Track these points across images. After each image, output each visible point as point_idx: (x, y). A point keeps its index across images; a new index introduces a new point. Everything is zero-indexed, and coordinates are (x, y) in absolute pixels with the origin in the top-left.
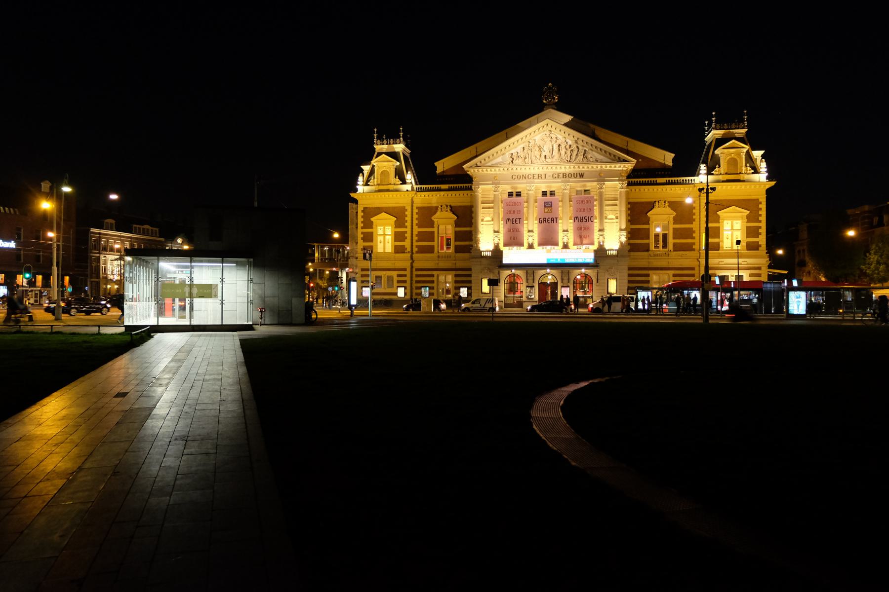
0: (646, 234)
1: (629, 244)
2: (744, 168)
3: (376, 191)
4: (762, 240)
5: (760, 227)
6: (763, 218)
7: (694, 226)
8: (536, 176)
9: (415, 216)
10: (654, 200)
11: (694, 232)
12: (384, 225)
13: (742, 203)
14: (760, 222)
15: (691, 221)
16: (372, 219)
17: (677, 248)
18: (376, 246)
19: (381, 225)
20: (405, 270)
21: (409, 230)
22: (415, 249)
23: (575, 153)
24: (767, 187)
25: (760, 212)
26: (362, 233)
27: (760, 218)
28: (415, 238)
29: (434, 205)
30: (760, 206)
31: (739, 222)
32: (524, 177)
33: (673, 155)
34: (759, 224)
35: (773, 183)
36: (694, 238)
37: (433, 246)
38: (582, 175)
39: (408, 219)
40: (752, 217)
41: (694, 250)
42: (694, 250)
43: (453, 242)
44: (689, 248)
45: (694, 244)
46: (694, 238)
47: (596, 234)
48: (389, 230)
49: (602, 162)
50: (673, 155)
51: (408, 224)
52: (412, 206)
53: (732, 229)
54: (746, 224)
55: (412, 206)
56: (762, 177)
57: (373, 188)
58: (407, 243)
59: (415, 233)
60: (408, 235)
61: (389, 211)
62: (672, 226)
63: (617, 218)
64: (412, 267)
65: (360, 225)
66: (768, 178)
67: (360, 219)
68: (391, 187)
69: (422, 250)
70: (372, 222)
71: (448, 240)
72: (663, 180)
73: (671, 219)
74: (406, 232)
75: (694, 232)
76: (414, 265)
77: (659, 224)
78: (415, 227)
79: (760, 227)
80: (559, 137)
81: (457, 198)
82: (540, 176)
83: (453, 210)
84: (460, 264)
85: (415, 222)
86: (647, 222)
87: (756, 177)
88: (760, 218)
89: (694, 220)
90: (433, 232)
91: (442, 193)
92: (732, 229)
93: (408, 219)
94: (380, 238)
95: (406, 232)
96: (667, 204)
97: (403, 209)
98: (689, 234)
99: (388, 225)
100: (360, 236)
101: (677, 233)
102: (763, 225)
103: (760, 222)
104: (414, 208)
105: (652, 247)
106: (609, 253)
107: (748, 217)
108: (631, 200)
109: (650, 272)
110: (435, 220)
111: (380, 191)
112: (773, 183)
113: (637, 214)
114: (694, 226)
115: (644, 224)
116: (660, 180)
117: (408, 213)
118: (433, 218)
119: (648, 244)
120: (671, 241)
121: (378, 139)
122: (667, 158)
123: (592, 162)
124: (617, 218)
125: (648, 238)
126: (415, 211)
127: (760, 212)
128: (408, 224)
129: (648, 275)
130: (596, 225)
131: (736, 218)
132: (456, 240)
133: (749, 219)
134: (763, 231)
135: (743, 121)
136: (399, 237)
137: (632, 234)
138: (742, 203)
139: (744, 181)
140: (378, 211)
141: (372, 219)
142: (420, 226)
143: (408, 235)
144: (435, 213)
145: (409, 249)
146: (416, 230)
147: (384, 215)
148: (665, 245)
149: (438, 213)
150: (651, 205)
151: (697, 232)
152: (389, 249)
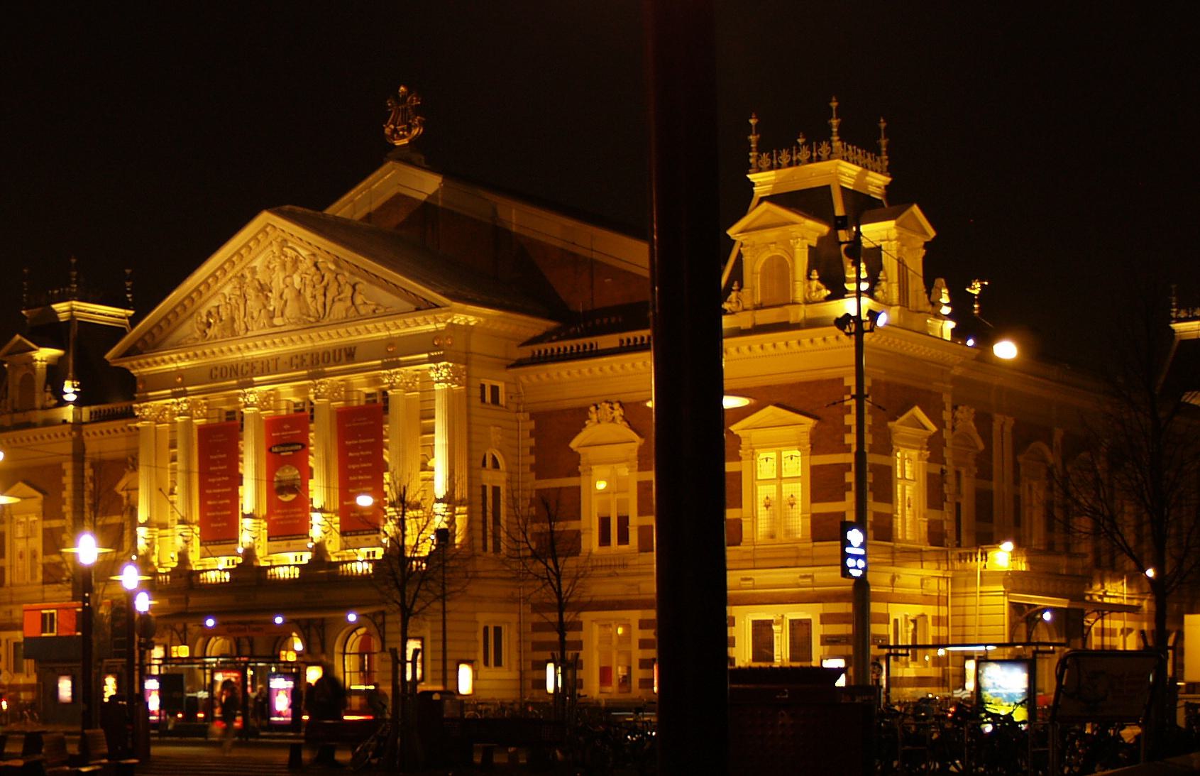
29: (122, 455)
86: (573, 465)
92: (780, 477)
126: (89, 472)
150: (577, 418)
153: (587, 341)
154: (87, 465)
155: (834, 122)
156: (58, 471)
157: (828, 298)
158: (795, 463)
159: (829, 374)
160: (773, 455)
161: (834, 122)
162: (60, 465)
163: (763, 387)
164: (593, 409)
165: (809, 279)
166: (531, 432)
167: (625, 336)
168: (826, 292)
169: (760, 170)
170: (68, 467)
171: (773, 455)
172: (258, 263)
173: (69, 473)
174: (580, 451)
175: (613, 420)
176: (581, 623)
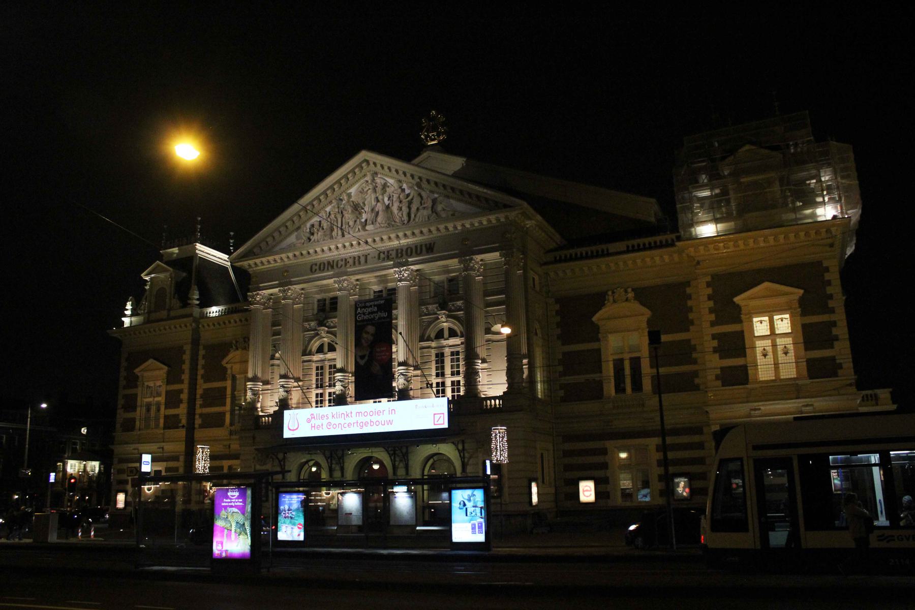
0: (595, 360)
4: (842, 351)
5: (834, 324)
6: (838, 301)
8: (351, 261)
9: (201, 362)
14: (832, 311)
15: (685, 324)
21: (185, 386)
22: (198, 421)
27: (831, 304)
28: (199, 402)
30: (827, 276)
32: (330, 265)
34: (833, 317)
36: (695, 362)
41: (696, 388)
42: (696, 388)
49: (464, 216)
51: (186, 377)
58: (182, 411)
59: (199, 392)
60: (184, 396)
72: (621, 246)
74: (181, 391)
75: (694, 349)
77: (624, 334)
78: (200, 381)
79: (834, 324)
80: (391, 181)
82: (356, 260)
85: (201, 372)
86: (594, 333)
88: (831, 304)
89: (692, 323)
90: (225, 388)
93: (186, 367)
95: (181, 391)
96: (631, 295)
98: (685, 353)
102: (840, 316)
103: (832, 311)
105: (610, 388)
107: (802, 302)
109: (609, 444)
110: (228, 366)
116: (613, 247)
117: (187, 357)
123: (447, 220)
126: (202, 352)
127: (829, 290)
128: (186, 377)
129: (604, 452)
134: (842, 331)
141: (136, 371)
142: (207, 379)
145: (184, 421)
148: (637, 386)
150: (598, 300)
153: (604, 247)
154: (201, 347)
156: (181, 350)
158: (783, 324)
160: (766, 318)
162: (182, 347)
164: (610, 293)
166: (557, 312)
170: (188, 348)
171: (766, 318)
172: (353, 190)
173: (188, 352)
175: (627, 300)
176: (606, 449)
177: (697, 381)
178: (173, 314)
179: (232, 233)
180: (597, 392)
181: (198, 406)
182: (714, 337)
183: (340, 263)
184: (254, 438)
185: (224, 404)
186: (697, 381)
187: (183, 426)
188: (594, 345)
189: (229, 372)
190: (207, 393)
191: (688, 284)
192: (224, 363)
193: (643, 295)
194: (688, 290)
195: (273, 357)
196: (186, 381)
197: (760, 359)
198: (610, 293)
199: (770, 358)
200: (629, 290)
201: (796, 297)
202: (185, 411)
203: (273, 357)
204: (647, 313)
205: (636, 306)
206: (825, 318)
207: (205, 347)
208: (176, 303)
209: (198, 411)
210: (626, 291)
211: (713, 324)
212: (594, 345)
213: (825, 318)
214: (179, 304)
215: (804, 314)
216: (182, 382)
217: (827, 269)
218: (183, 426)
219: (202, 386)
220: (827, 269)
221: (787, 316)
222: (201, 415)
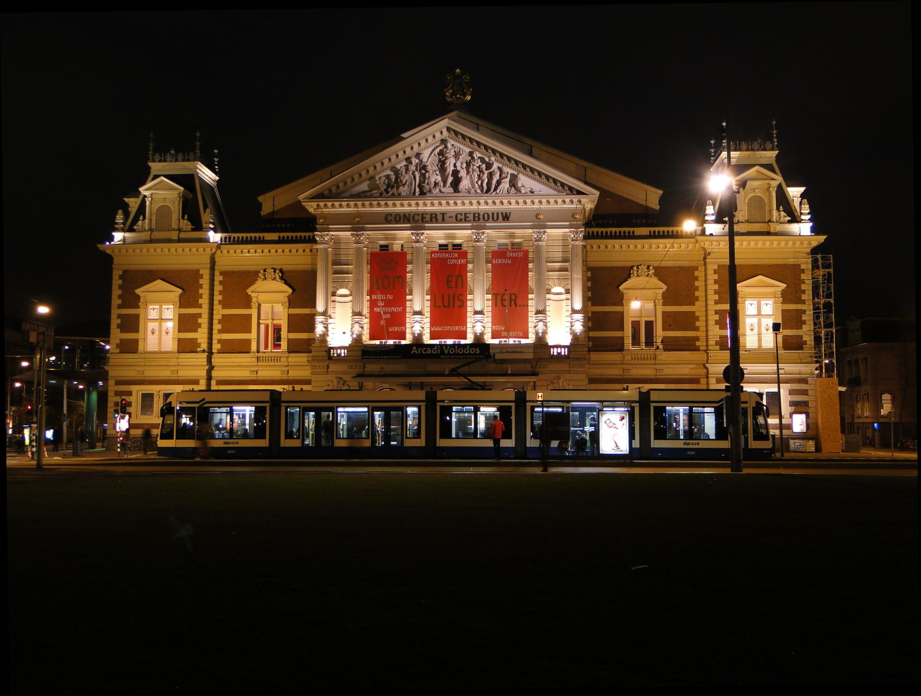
0: (618, 321)
1: (590, 339)
2: (775, 213)
3: (146, 242)
4: (807, 332)
5: (804, 312)
7: (697, 308)
8: (428, 217)
9: (218, 288)
10: (630, 264)
11: (697, 319)
12: (161, 302)
13: (774, 271)
15: (692, 300)
16: (138, 291)
17: (671, 345)
18: (145, 339)
19: (154, 302)
20: (196, 382)
21: (204, 311)
22: (216, 347)
23: (496, 178)
24: (815, 244)
25: (803, 287)
26: (119, 316)
28: (217, 326)
31: (770, 302)
33: (661, 192)
35: (822, 238)
36: (697, 329)
37: (249, 342)
38: (506, 217)
39: (205, 291)
40: (790, 295)
42: (697, 349)
43: (284, 333)
44: (689, 345)
45: (697, 339)
46: (697, 329)
47: (532, 319)
48: (170, 312)
50: (661, 192)
51: (204, 301)
52: (212, 269)
53: (760, 316)
54: (781, 307)
55: (212, 269)
56: (804, 228)
57: (145, 236)
58: (201, 336)
59: (217, 317)
61: (170, 277)
62: (660, 309)
63: (567, 292)
64: (209, 378)
65: (116, 301)
66: (813, 230)
67: (116, 292)
68: (174, 235)
69: (230, 348)
70: (138, 297)
71: (277, 329)
72: (644, 231)
73: (660, 296)
74: (200, 315)
75: (697, 319)
76: (214, 373)
78: (217, 307)
79: (804, 312)
81: (293, 256)
83: (285, 277)
84: (294, 374)
85: (218, 297)
86: (620, 300)
87: (795, 228)
88: (804, 297)
89: (697, 299)
90: (250, 316)
91: (266, 247)
92: (759, 314)
93: (205, 291)
94: (151, 326)
95: (200, 315)
97: (196, 275)
98: (689, 321)
99: (167, 302)
100: (115, 321)
101: (670, 321)
104: (217, 273)
106: (555, 351)
107: (784, 294)
108: (590, 264)
110: (253, 295)
111: (151, 241)
112: (822, 238)
113: (603, 288)
114: (697, 308)
115: (614, 305)
116: (639, 231)
117: (205, 282)
118: (249, 291)
119: (622, 338)
120: (660, 333)
121: (155, 152)
122: (652, 197)
123: (525, 194)
124: (567, 292)
125: (621, 328)
126: (218, 278)
130: (532, 306)
131: (766, 296)
132: (290, 330)
133: (786, 297)
135: (771, 139)
136: (186, 323)
137: (594, 321)
138: (774, 271)
139: (776, 234)
140: (149, 276)
142: (225, 304)
143: (204, 321)
144: (253, 283)
145: (204, 346)
146: (219, 312)
147: (159, 284)
148: (650, 342)
149: (260, 285)
150: (626, 273)
151: (703, 319)
152: (169, 344)
155: (198, 143)
156: (196, 275)
157: (789, 222)
159: (791, 261)
160: (755, 302)
161: (151, 145)
163: (774, 265)
164: (635, 268)
165: (778, 209)
167: (652, 229)
168: (788, 218)
169: (154, 161)
170: (206, 273)
174: (625, 291)
177: (698, 343)
178: (183, 235)
179: (216, 151)
180: (618, 346)
181: (215, 332)
182: (716, 312)
183: (417, 218)
184: (328, 367)
185: (250, 332)
186: (698, 343)
187: (204, 351)
188: (617, 309)
189: (254, 300)
190: (225, 319)
191: (696, 268)
192: (249, 291)
193: (661, 273)
194: (696, 273)
195: (334, 294)
196: (206, 306)
197: (748, 332)
198: (635, 268)
199: (756, 331)
200: (651, 268)
201: (780, 289)
202: (206, 336)
203: (334, 294)
204: (665, 287)
205: (655, 281)
206: (800, 307)
207: (221, 273)
208: (186, 224)
209: (216, 336)
210: (648, 268)
211: (716, 302)
212: (617, 309)
213: (800, 307)
214: (190, 227)
215: (784, 302)
216: (200, 307)
217: (803, 271)
218: (204, 351)
219: (219, 312)
220: (803, 271)
221: (771, 302)
222: (219, 341)
